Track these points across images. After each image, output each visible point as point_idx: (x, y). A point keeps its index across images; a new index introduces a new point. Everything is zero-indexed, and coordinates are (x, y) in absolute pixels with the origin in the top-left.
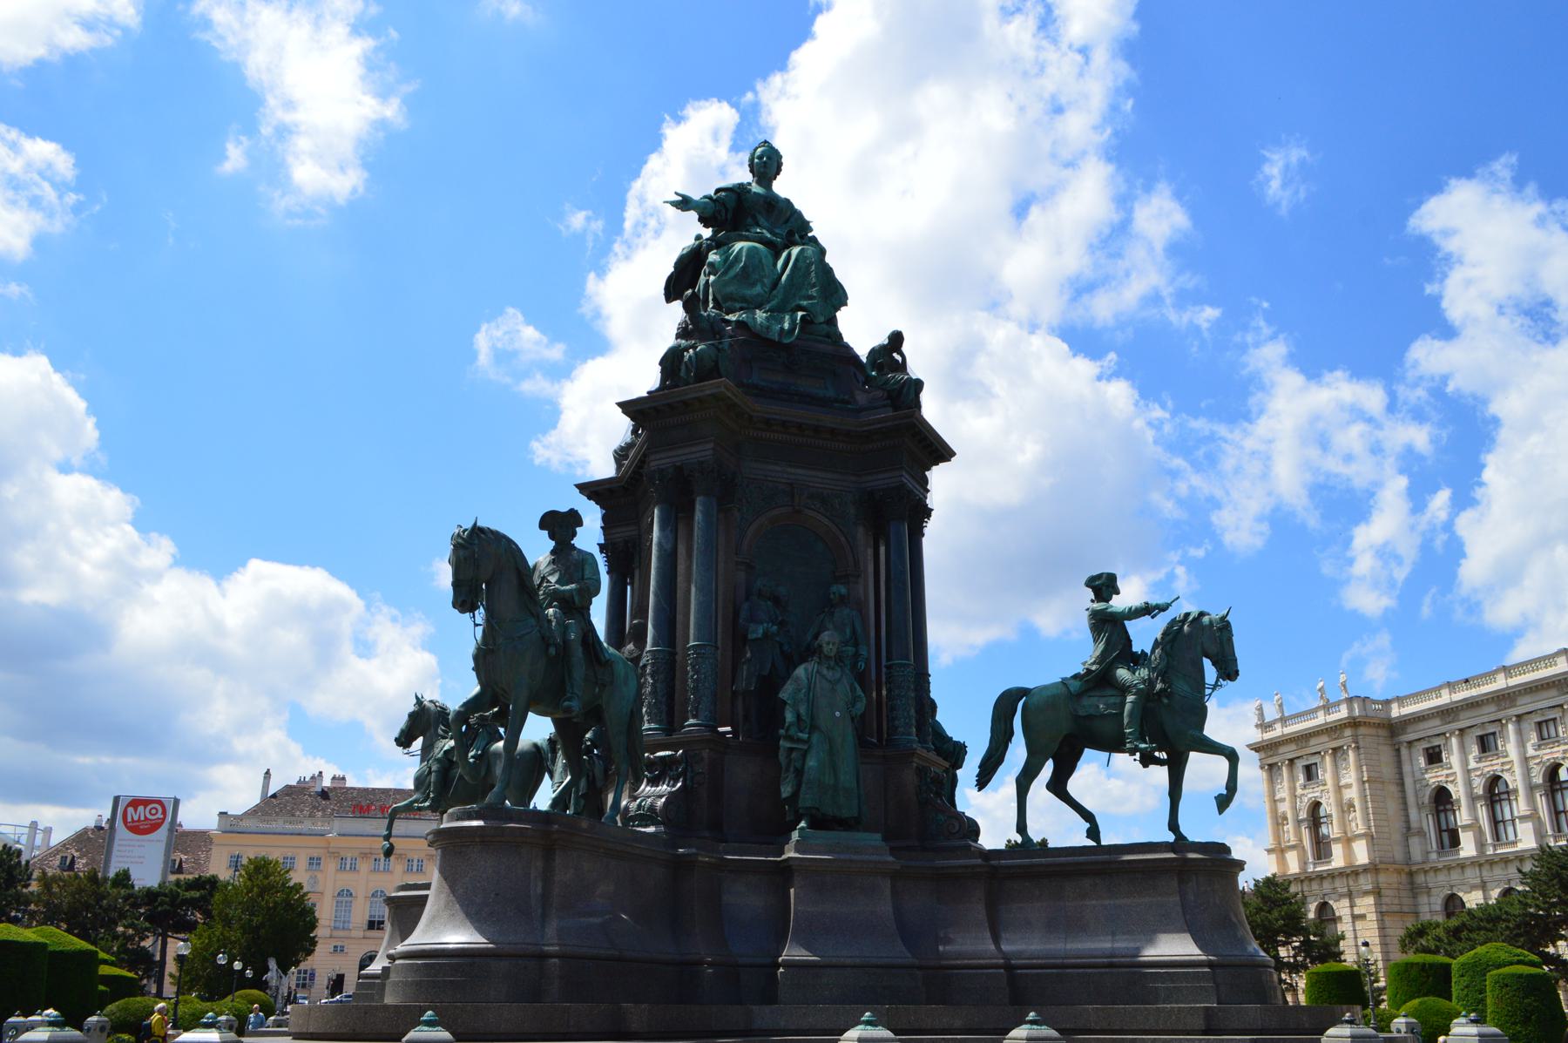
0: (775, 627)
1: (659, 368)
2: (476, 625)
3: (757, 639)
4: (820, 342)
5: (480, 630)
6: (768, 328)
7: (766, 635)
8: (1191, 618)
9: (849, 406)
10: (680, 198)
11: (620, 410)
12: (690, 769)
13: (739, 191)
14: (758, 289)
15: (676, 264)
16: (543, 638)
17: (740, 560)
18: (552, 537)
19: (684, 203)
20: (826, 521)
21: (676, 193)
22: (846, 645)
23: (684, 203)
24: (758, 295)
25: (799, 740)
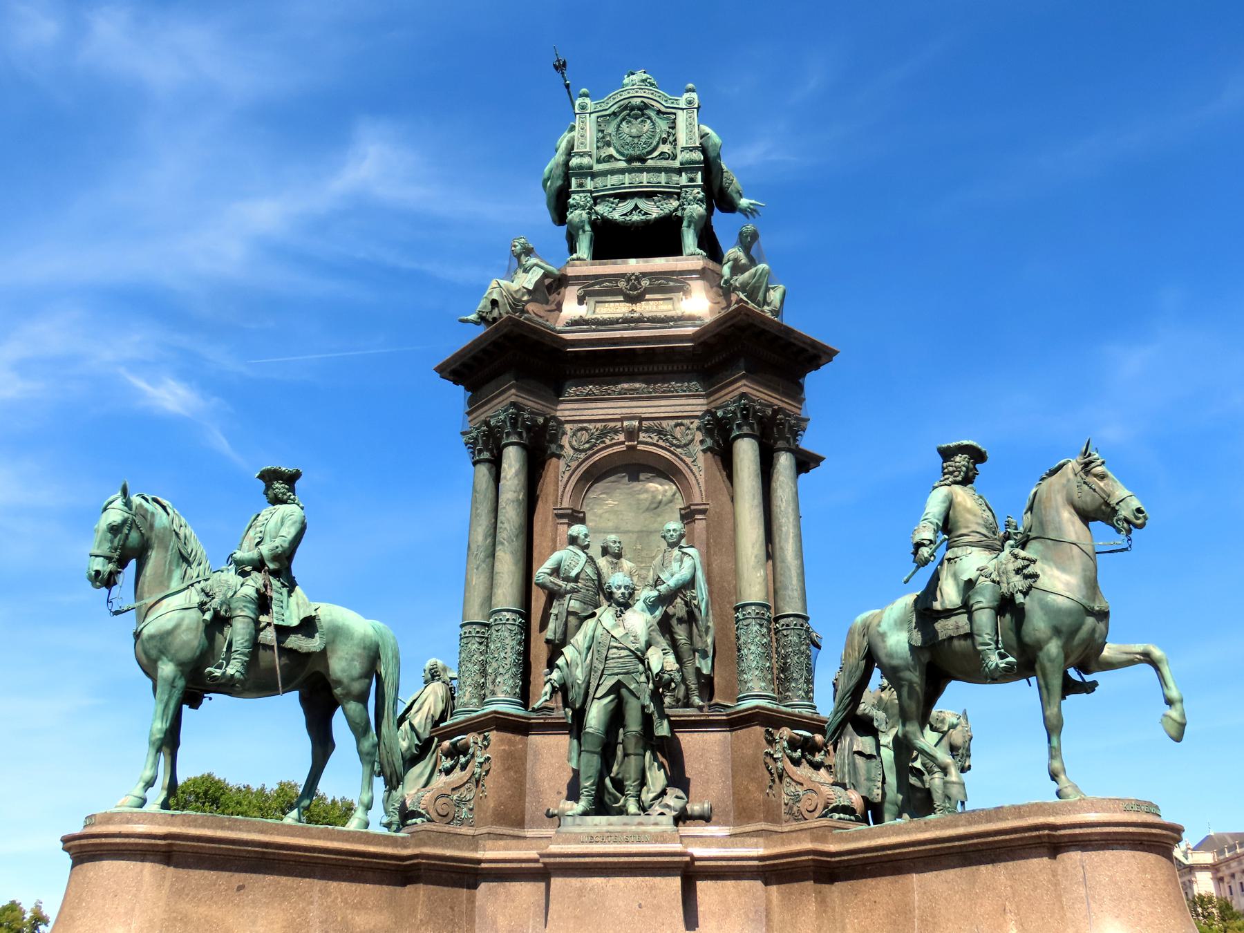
17: (559, 512)
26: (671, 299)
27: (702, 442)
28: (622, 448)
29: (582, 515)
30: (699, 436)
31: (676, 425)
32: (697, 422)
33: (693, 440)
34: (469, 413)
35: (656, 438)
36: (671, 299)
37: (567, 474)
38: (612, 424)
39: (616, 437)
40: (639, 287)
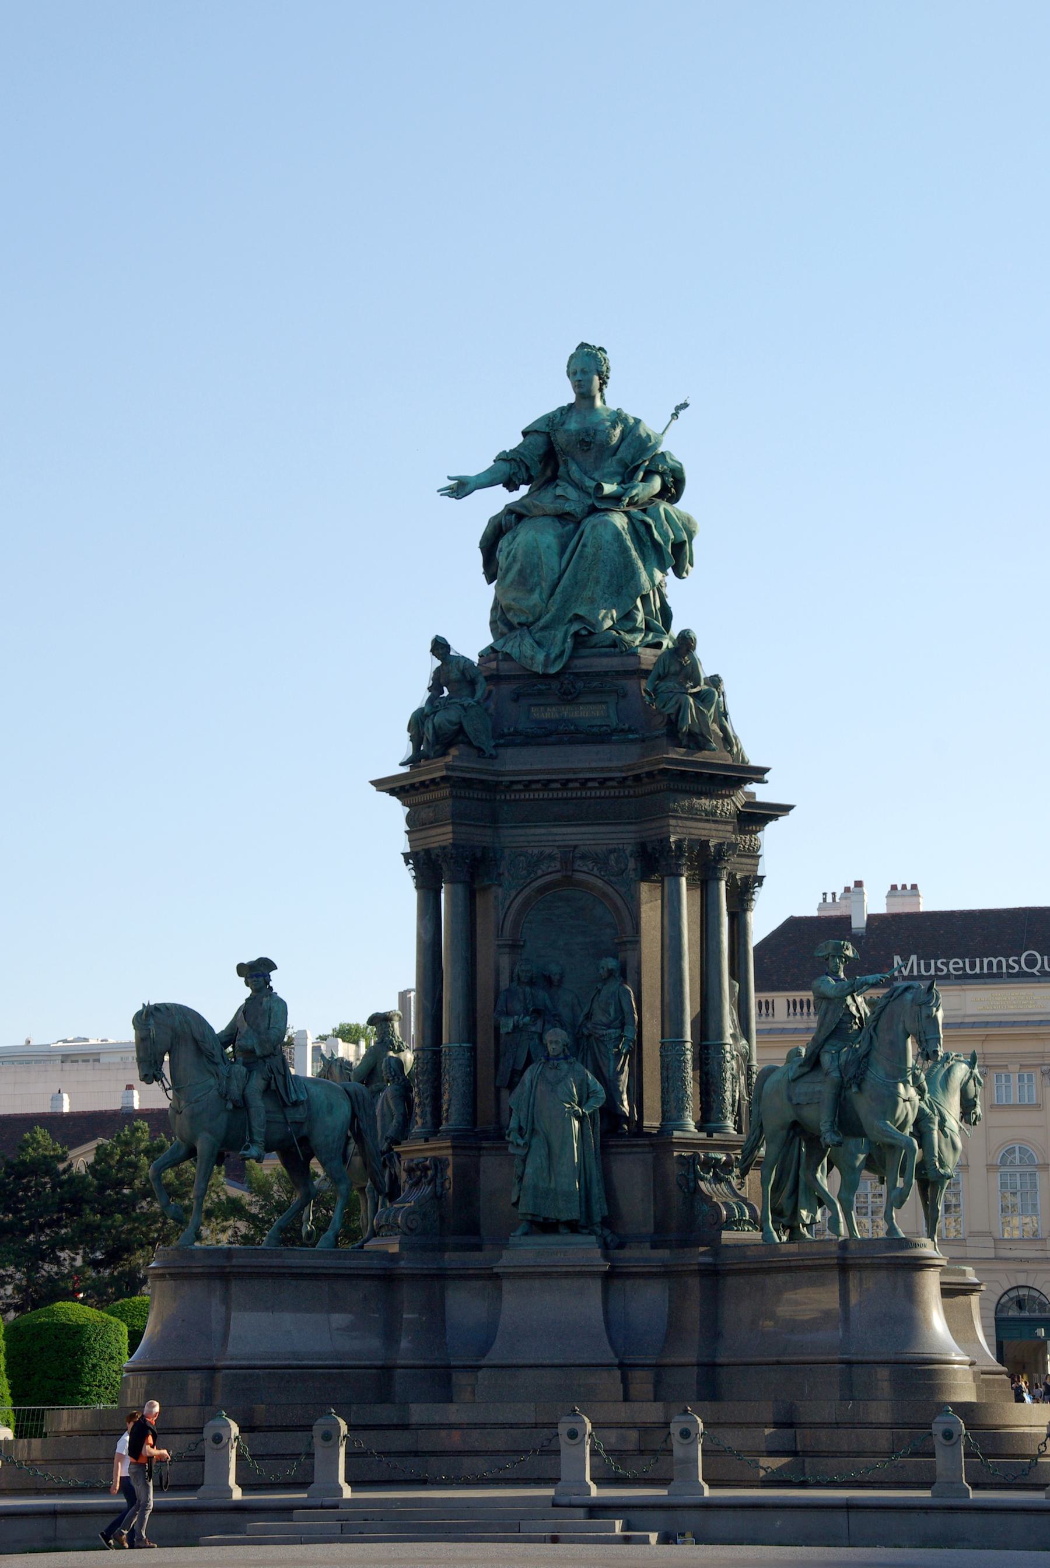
0: (528, 1018)
1: (407, 735)
2: (166, 1090)
3: (508, 1033)
4: (606, 655)
5: (170, 1093)
6: (532, 658)
7: (516, 1027)
8: (895, 994)
9: (631, 736)
10: (456, 481)
11: (374, 788)
12: (439, 1175)
13: (547, 430)
14: (535, 597)
15: (481, 543)
16: (220, 1094)
17: (500, 943)
18: (247, 984)
19: (460, 488)
20: (599, 883)
21: (450, 478)
22: (609, 1028)
23: (460, 488)
24: (535, 605)
25: (518, 1145)
26: (606, 703)
27: (634, 870)
28: (558, 876)
29: (522, 943)
30: (632, 864)
31: (611, 851)
32: (629, 849)
33: (626, 869)
34: (406, 832)
35: (591, 868)
36: (606, 703)
37: (508, 902)
38: (548, 851)
39: (553, 865)
40: (572, 691)
